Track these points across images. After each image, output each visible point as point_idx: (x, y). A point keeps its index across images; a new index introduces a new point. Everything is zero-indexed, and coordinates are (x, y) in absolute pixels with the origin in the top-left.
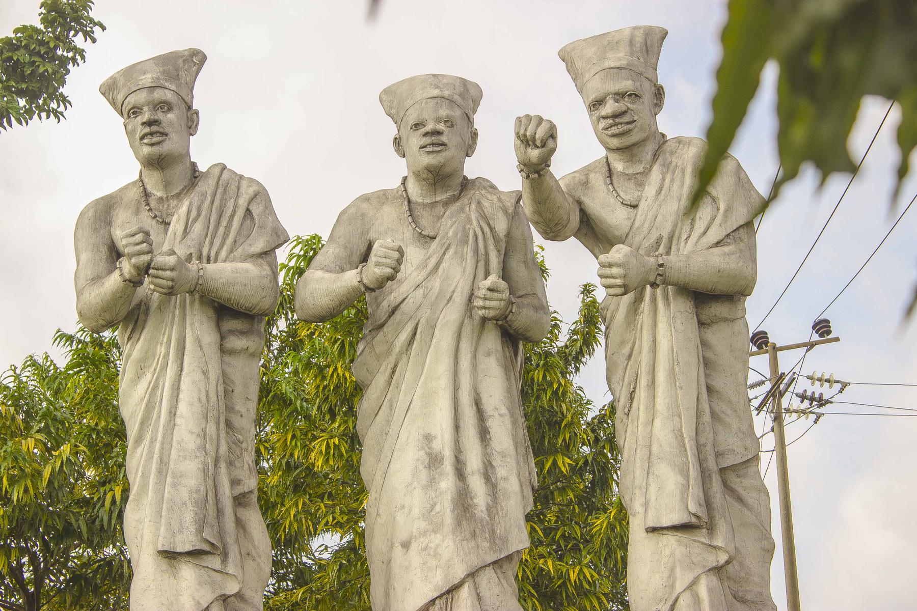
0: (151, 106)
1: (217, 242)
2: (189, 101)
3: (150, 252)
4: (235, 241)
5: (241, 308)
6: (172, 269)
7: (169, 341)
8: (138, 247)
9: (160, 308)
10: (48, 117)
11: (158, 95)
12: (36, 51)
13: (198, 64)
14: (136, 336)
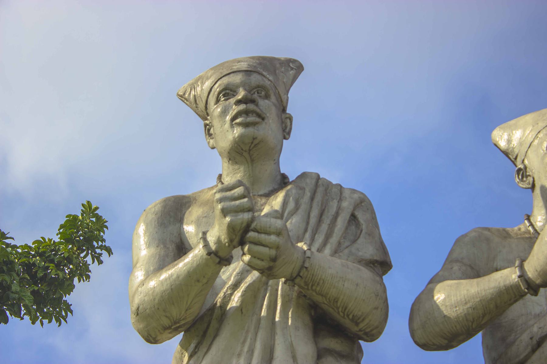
0: (247, 88)
1: (320, 239)
2: (284, 101)
3: (250, 210)
4: (339, 243)
5: (348, 316)
6: (278, 234)
7: (251, 351)
8: (238, 202)
9: (240, 309)
10: (50, 322)
11: (255, 79)
12: (51, 258)
13: (295, 69)
14: (203, 349)
